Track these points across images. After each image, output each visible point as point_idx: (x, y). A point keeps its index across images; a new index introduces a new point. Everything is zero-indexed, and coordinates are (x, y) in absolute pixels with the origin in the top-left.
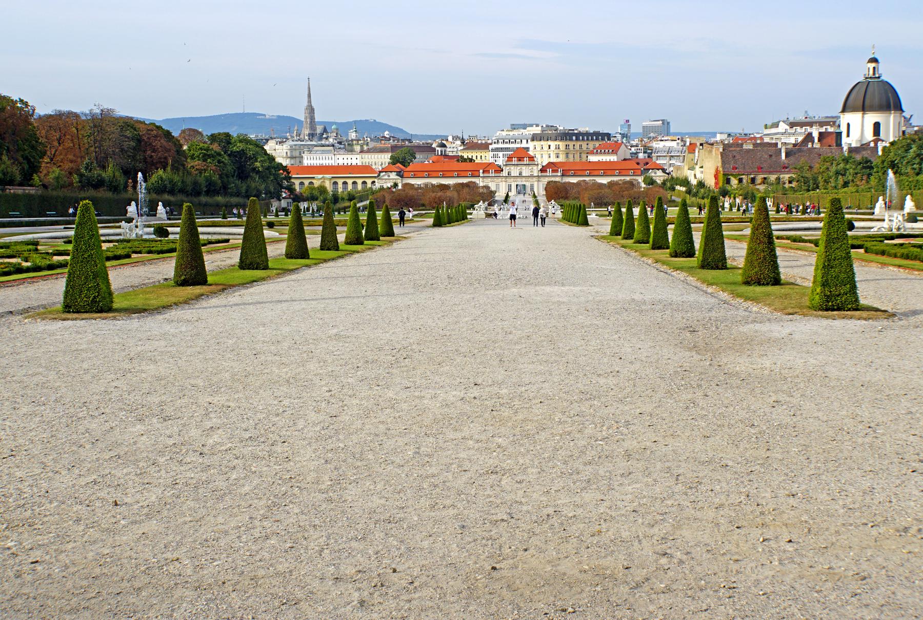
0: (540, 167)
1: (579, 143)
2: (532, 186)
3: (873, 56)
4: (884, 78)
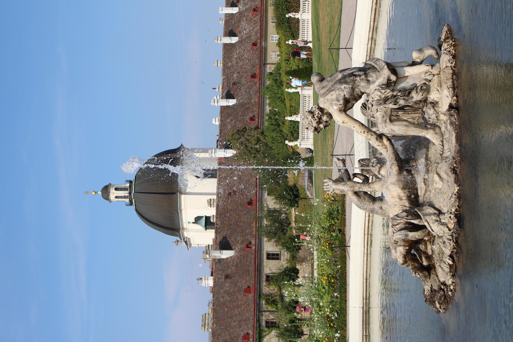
3: (100, 193)
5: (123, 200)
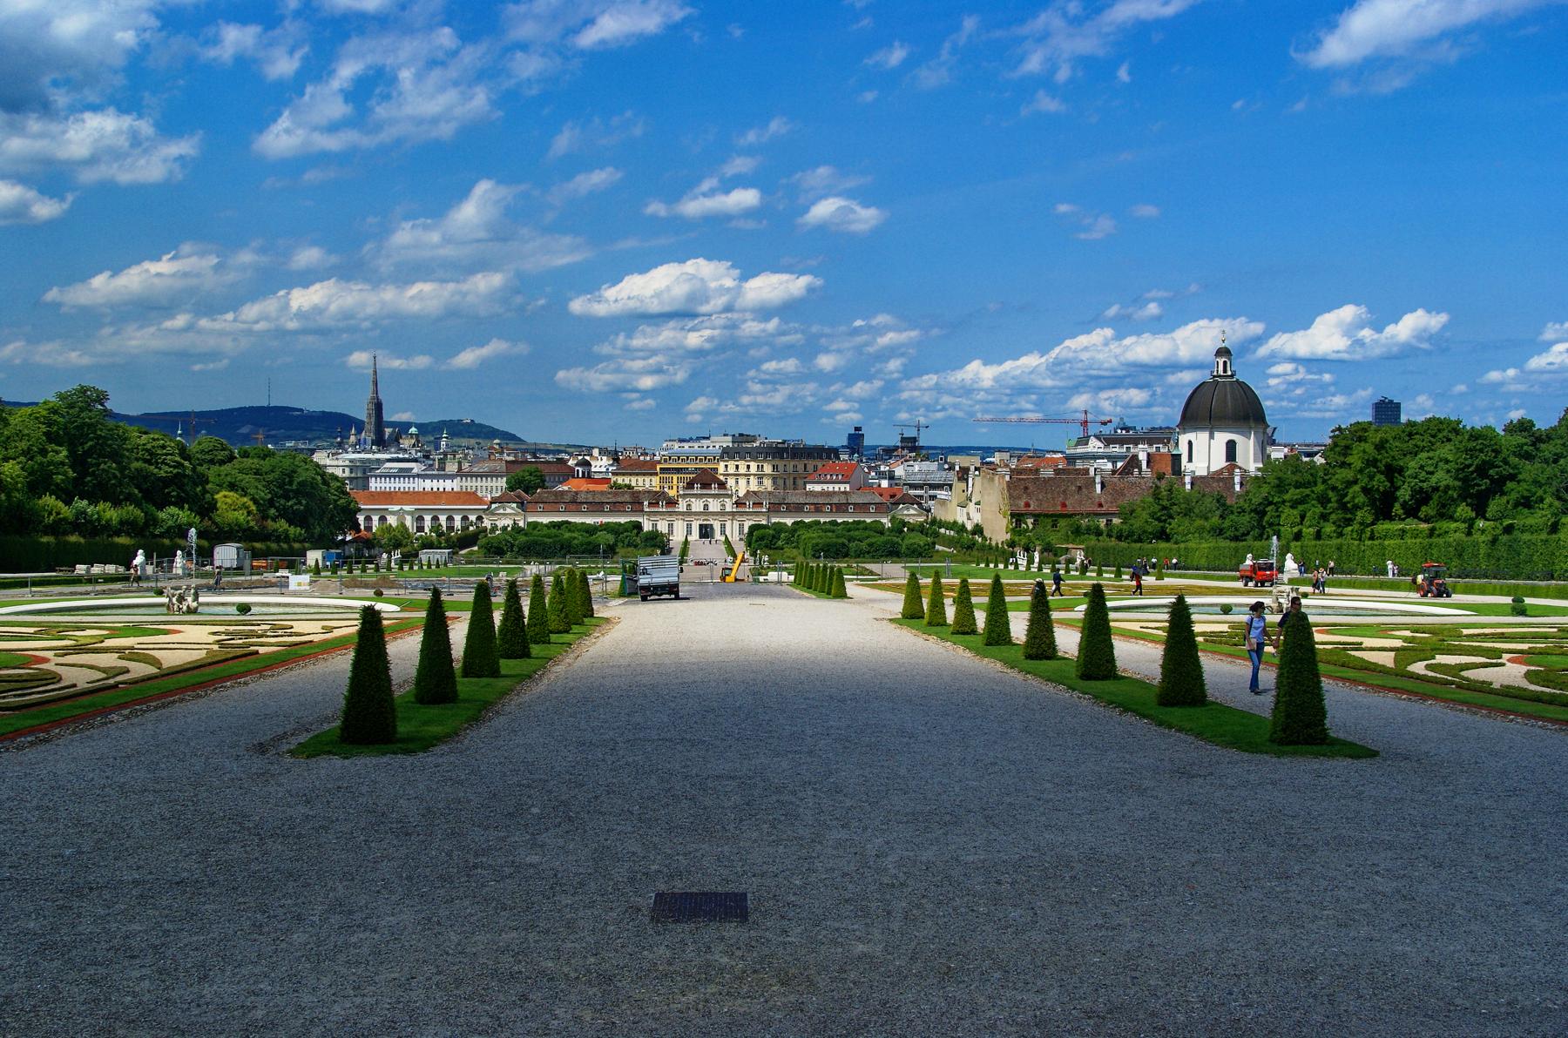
0: (734, 500)
1: (792, 463)
2: (723, 527)
4: (1239, 377)
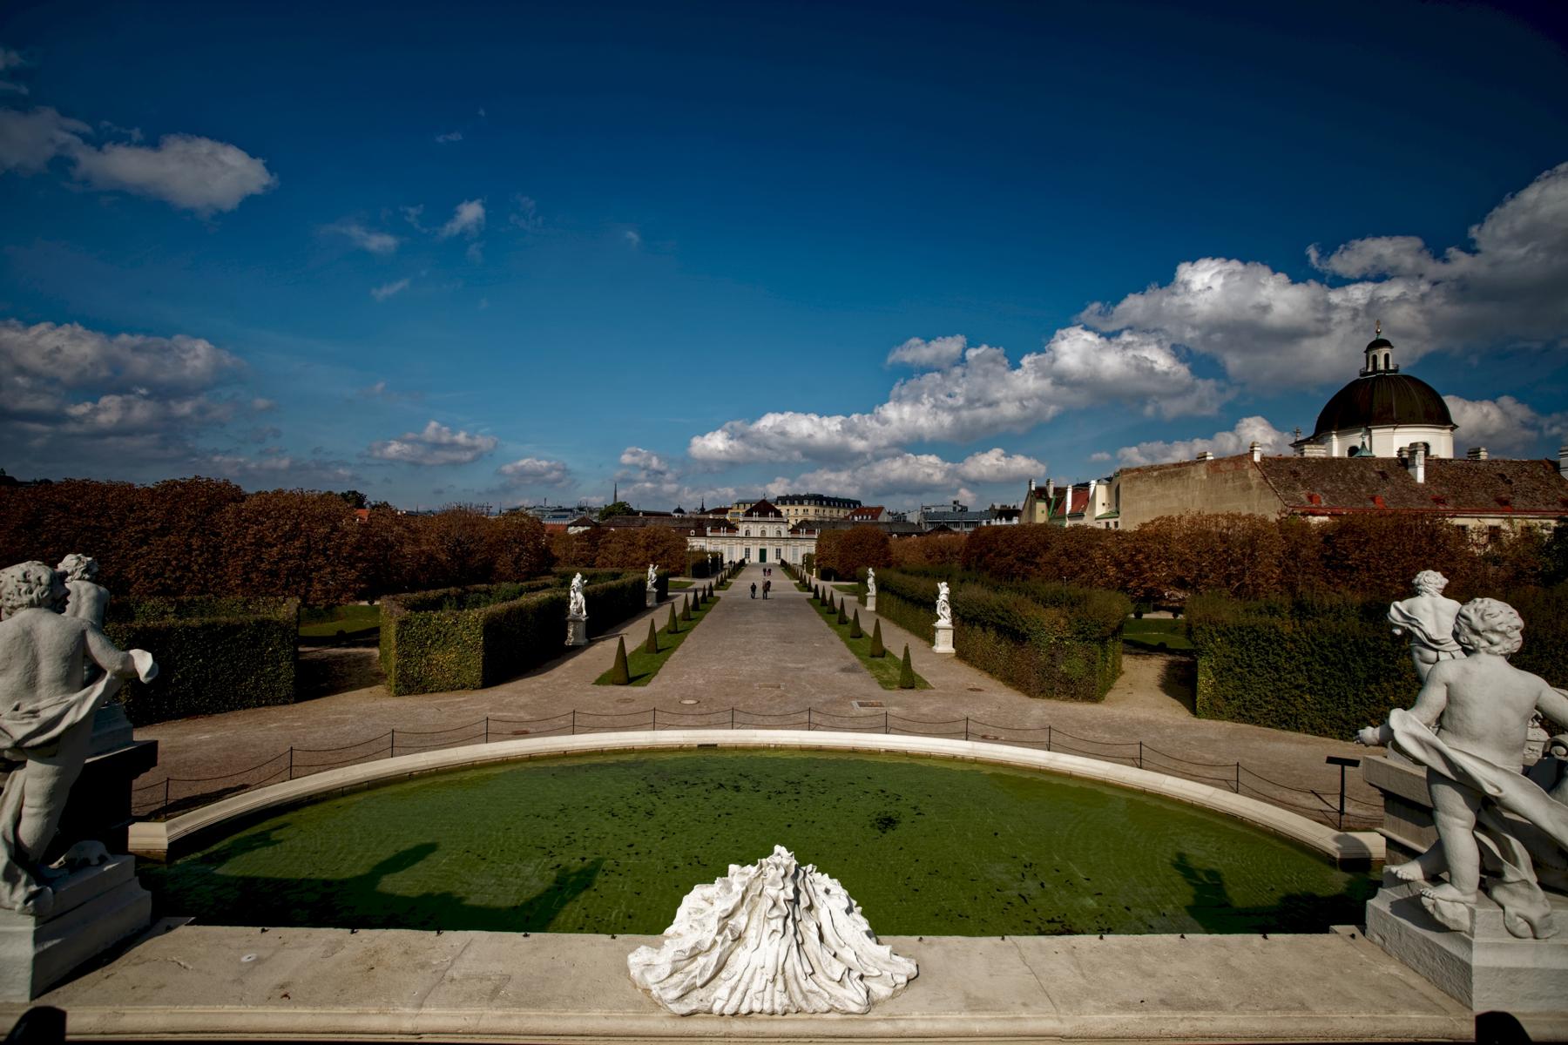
0: (790, 527)
2: (778, 552)
5: (1371, 365)
